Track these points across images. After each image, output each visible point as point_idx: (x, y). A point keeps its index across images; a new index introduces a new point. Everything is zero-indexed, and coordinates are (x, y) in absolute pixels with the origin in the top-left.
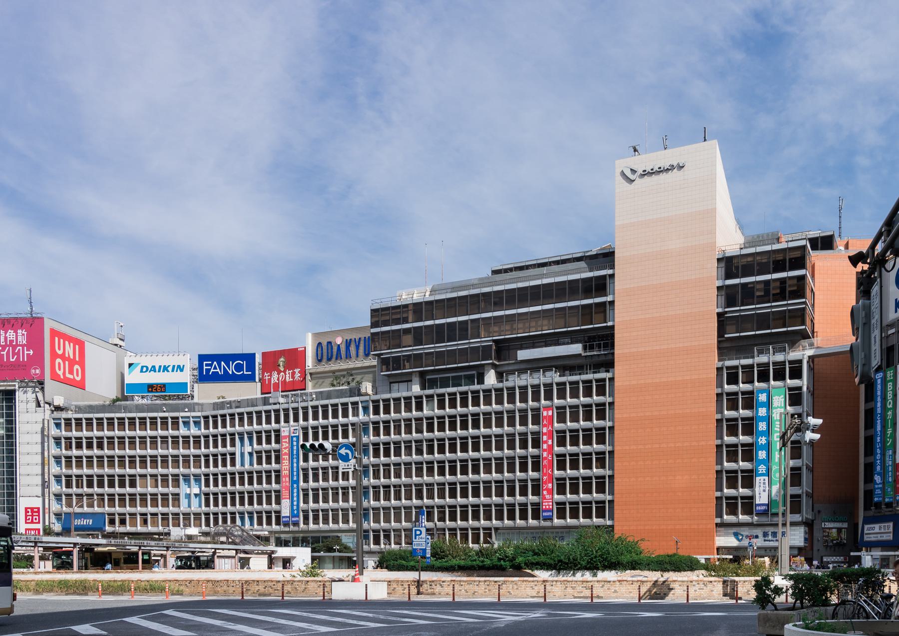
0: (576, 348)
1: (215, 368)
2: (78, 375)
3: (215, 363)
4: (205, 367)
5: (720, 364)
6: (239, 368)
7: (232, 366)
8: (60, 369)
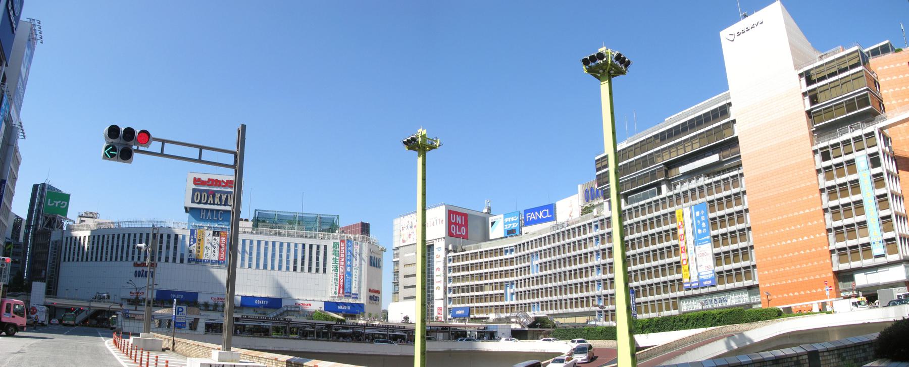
1: (533, 216)
2: (463, 232)
3: (532, 214)
4: (527, 217)
6: (545, 214)
7: (541, 214)
8: (453, 230)
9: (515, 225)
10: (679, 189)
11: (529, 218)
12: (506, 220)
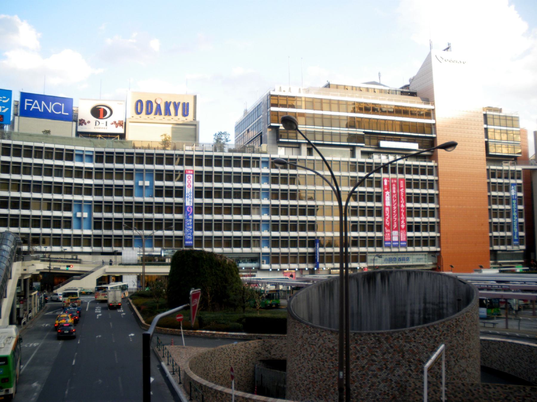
0: (414, 146)
3: (36, 101)
4: (26, 104)
5: (488, 167)
10: (376, 159)
11: (29, 107)
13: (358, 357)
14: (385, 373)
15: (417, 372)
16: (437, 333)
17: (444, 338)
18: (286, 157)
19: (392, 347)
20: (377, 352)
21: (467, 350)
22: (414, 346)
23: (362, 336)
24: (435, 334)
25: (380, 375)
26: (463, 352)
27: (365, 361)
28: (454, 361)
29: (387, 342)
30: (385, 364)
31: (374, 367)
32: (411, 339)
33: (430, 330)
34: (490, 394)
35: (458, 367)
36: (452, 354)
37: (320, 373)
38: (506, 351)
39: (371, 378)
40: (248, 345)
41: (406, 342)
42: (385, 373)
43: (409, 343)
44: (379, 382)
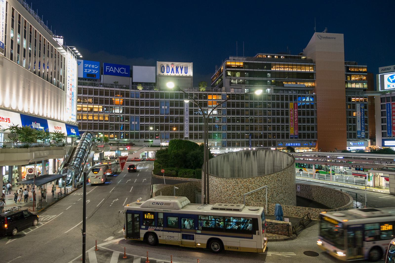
3: (112, 67)
4: (107, 69)
6: (122, 70)
9: (95, 71)
11: (108, 70)
12: (87, 65)
13: (228, 190)
14: (240, 198)
15: (256, 198)
16: (266, 180)
17: (270, 183)
18: (235, 93)
19: (243, 186)
20: (236, 188)
21: (284, 189)
22: (254, 186)
23: (229, 180)
24: (265, 181)
25: (238, 199)
26: (281, 190)
27: (231, 192)
28: (276, 194)
29: (241, 183)
30: (240, 194)
31: (235, 195)
32: (252, 182)
33: (262, 178)
34: (289, 211)
35: (278, 197)
36: (275, 191)
37: (212, 197)
38: (320, 192)
39: (233, 200)
40: (192, 184)
41: (250, 184)
42: (240, 198)
43: (252, 184)
44: (237, 202)
